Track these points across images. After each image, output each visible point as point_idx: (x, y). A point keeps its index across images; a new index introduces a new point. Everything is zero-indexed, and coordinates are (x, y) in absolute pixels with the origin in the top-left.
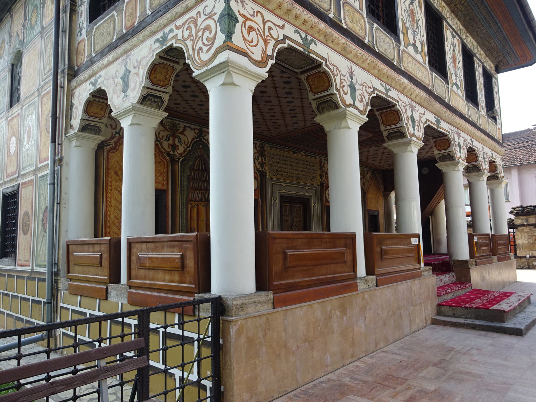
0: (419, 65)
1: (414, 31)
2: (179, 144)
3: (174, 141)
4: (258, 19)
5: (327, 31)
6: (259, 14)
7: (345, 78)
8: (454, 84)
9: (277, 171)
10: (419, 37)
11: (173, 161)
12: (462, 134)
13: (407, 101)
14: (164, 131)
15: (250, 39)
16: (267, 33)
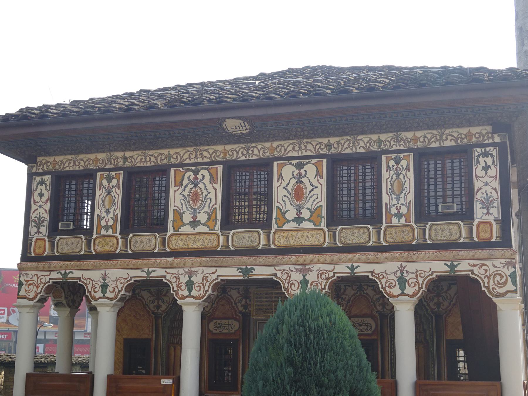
0: (198, 237)
1: (195, 210)
2: (162, 304)
3: (158, 303)
4: (35, 278)
5: (77, 264)
6: (36, 276)
7: (98, 282)
8: (288, 221)
9: (267, 309)
10: (206, 209)
11: (157, 317)
12: (316, 268)
13: (181, 271)
14: (151, 297)
15: (28, 290)
16: (39, 282)
